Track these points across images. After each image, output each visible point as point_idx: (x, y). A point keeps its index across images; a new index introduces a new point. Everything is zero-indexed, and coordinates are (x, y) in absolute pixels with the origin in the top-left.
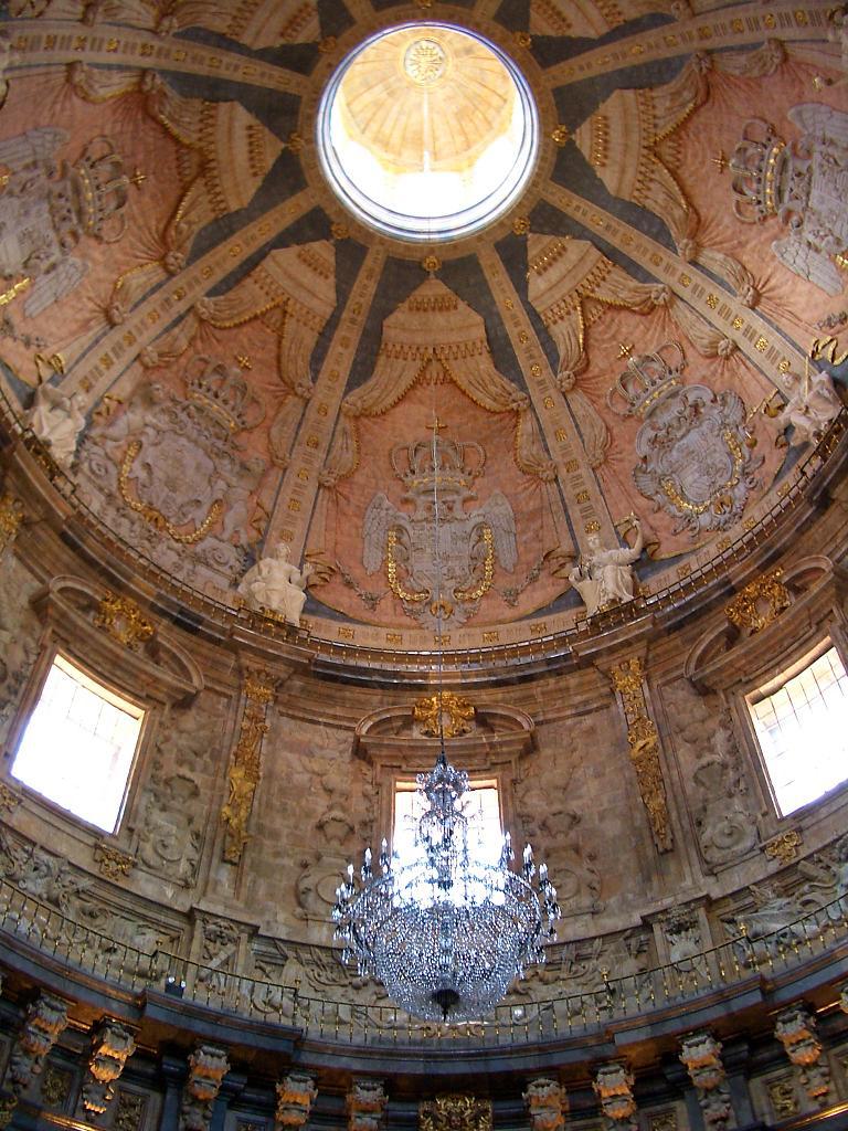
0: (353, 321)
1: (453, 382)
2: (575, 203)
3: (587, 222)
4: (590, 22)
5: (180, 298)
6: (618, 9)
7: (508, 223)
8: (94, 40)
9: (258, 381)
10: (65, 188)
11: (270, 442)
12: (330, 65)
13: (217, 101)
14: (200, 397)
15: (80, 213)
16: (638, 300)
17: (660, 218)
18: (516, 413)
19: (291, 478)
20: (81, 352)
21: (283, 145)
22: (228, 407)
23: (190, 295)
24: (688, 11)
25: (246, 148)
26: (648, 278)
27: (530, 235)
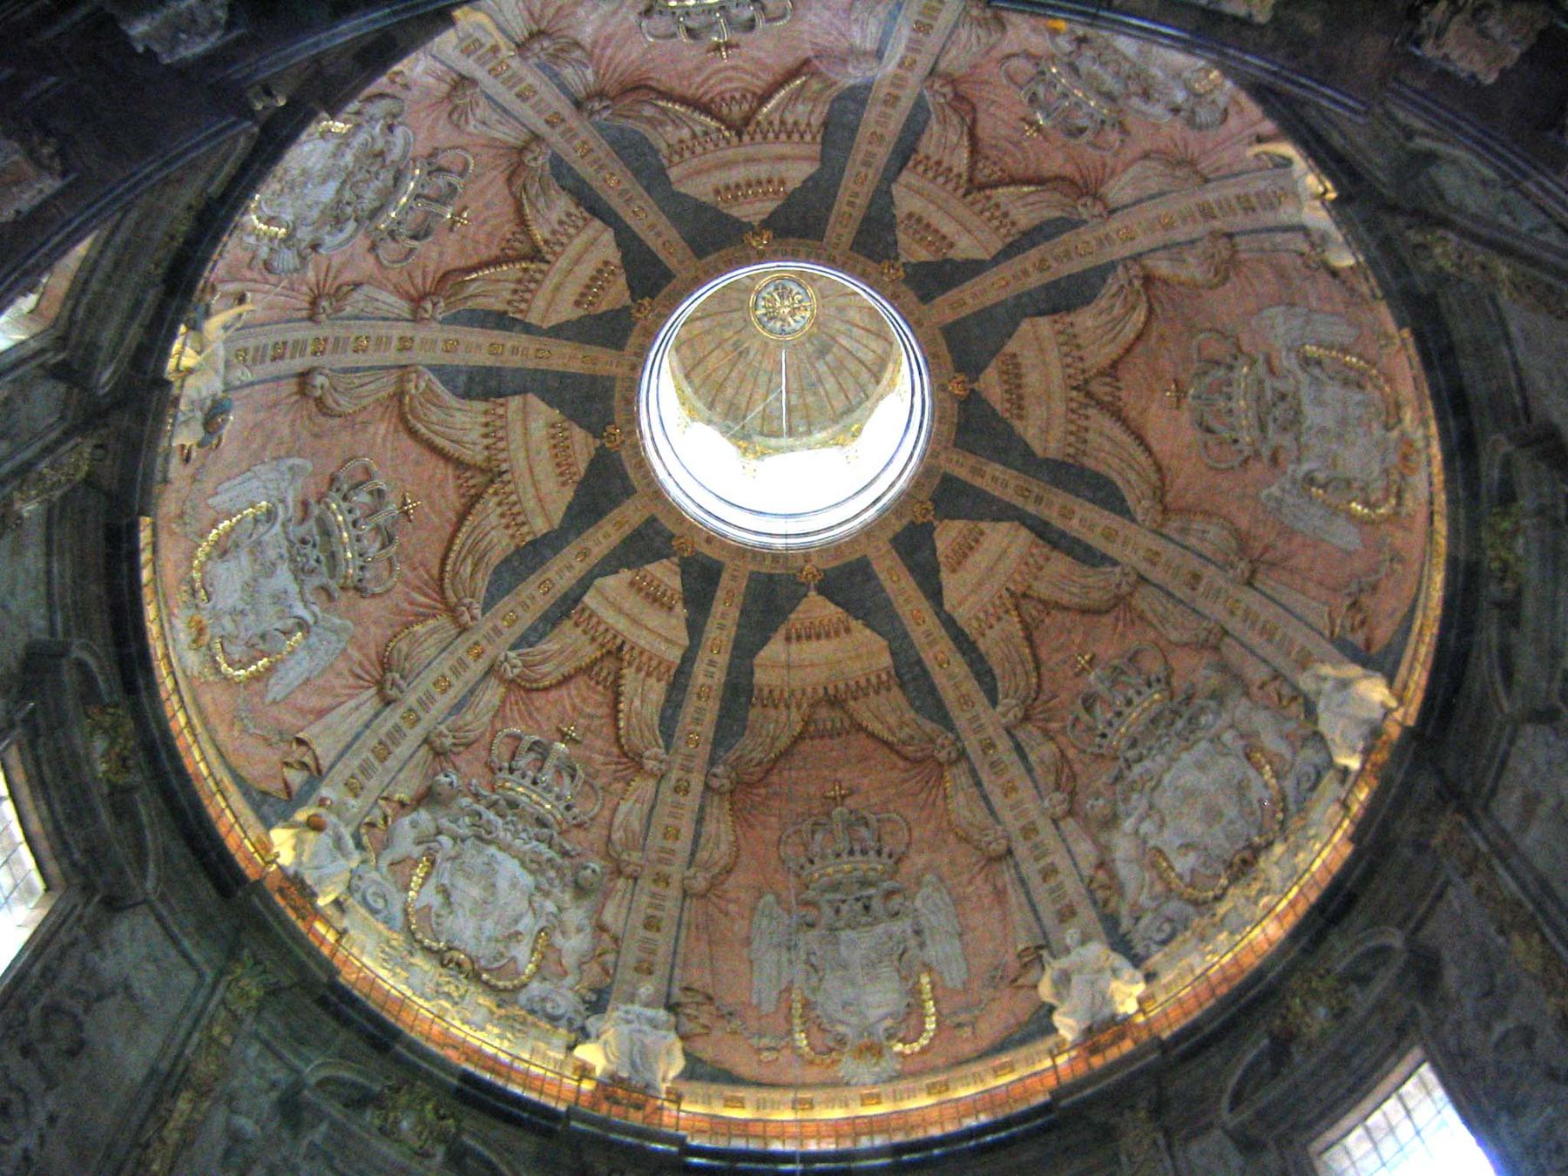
0: (1039, 499)
1: (1114, 365)
2: (846, 208)
3: (867, 189)
4: (594, 241)
5: (993, 745)
6: (564, 218)
7: (889, 291)
8: (660, 861)
9: (1109, 644)
10: (830, 902)
11: (1186, 645)
12: (709, 540)
13: (750, 684)
14: (1117, 739)
15: (865, 883)
16: (955, 120)
17: (832, 106)
18: (1148, 280)
19: (1234, 625)
20: (1027, 908)
21: (812, 593)
22: (1136, 700)
23: (990, 731)
24: (534, 146)
25: (814, 644)
26: (920, 106)
27: (903, 260)
